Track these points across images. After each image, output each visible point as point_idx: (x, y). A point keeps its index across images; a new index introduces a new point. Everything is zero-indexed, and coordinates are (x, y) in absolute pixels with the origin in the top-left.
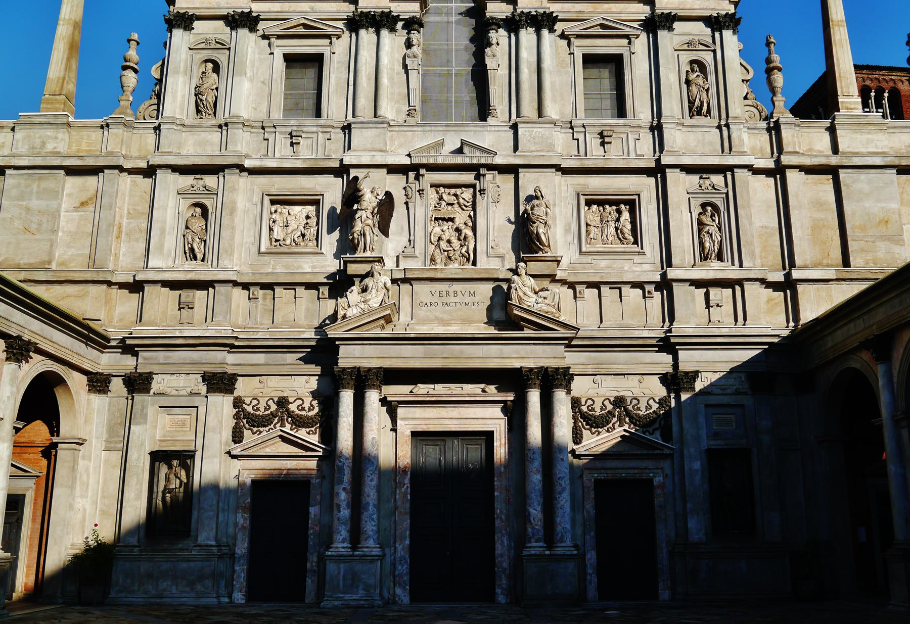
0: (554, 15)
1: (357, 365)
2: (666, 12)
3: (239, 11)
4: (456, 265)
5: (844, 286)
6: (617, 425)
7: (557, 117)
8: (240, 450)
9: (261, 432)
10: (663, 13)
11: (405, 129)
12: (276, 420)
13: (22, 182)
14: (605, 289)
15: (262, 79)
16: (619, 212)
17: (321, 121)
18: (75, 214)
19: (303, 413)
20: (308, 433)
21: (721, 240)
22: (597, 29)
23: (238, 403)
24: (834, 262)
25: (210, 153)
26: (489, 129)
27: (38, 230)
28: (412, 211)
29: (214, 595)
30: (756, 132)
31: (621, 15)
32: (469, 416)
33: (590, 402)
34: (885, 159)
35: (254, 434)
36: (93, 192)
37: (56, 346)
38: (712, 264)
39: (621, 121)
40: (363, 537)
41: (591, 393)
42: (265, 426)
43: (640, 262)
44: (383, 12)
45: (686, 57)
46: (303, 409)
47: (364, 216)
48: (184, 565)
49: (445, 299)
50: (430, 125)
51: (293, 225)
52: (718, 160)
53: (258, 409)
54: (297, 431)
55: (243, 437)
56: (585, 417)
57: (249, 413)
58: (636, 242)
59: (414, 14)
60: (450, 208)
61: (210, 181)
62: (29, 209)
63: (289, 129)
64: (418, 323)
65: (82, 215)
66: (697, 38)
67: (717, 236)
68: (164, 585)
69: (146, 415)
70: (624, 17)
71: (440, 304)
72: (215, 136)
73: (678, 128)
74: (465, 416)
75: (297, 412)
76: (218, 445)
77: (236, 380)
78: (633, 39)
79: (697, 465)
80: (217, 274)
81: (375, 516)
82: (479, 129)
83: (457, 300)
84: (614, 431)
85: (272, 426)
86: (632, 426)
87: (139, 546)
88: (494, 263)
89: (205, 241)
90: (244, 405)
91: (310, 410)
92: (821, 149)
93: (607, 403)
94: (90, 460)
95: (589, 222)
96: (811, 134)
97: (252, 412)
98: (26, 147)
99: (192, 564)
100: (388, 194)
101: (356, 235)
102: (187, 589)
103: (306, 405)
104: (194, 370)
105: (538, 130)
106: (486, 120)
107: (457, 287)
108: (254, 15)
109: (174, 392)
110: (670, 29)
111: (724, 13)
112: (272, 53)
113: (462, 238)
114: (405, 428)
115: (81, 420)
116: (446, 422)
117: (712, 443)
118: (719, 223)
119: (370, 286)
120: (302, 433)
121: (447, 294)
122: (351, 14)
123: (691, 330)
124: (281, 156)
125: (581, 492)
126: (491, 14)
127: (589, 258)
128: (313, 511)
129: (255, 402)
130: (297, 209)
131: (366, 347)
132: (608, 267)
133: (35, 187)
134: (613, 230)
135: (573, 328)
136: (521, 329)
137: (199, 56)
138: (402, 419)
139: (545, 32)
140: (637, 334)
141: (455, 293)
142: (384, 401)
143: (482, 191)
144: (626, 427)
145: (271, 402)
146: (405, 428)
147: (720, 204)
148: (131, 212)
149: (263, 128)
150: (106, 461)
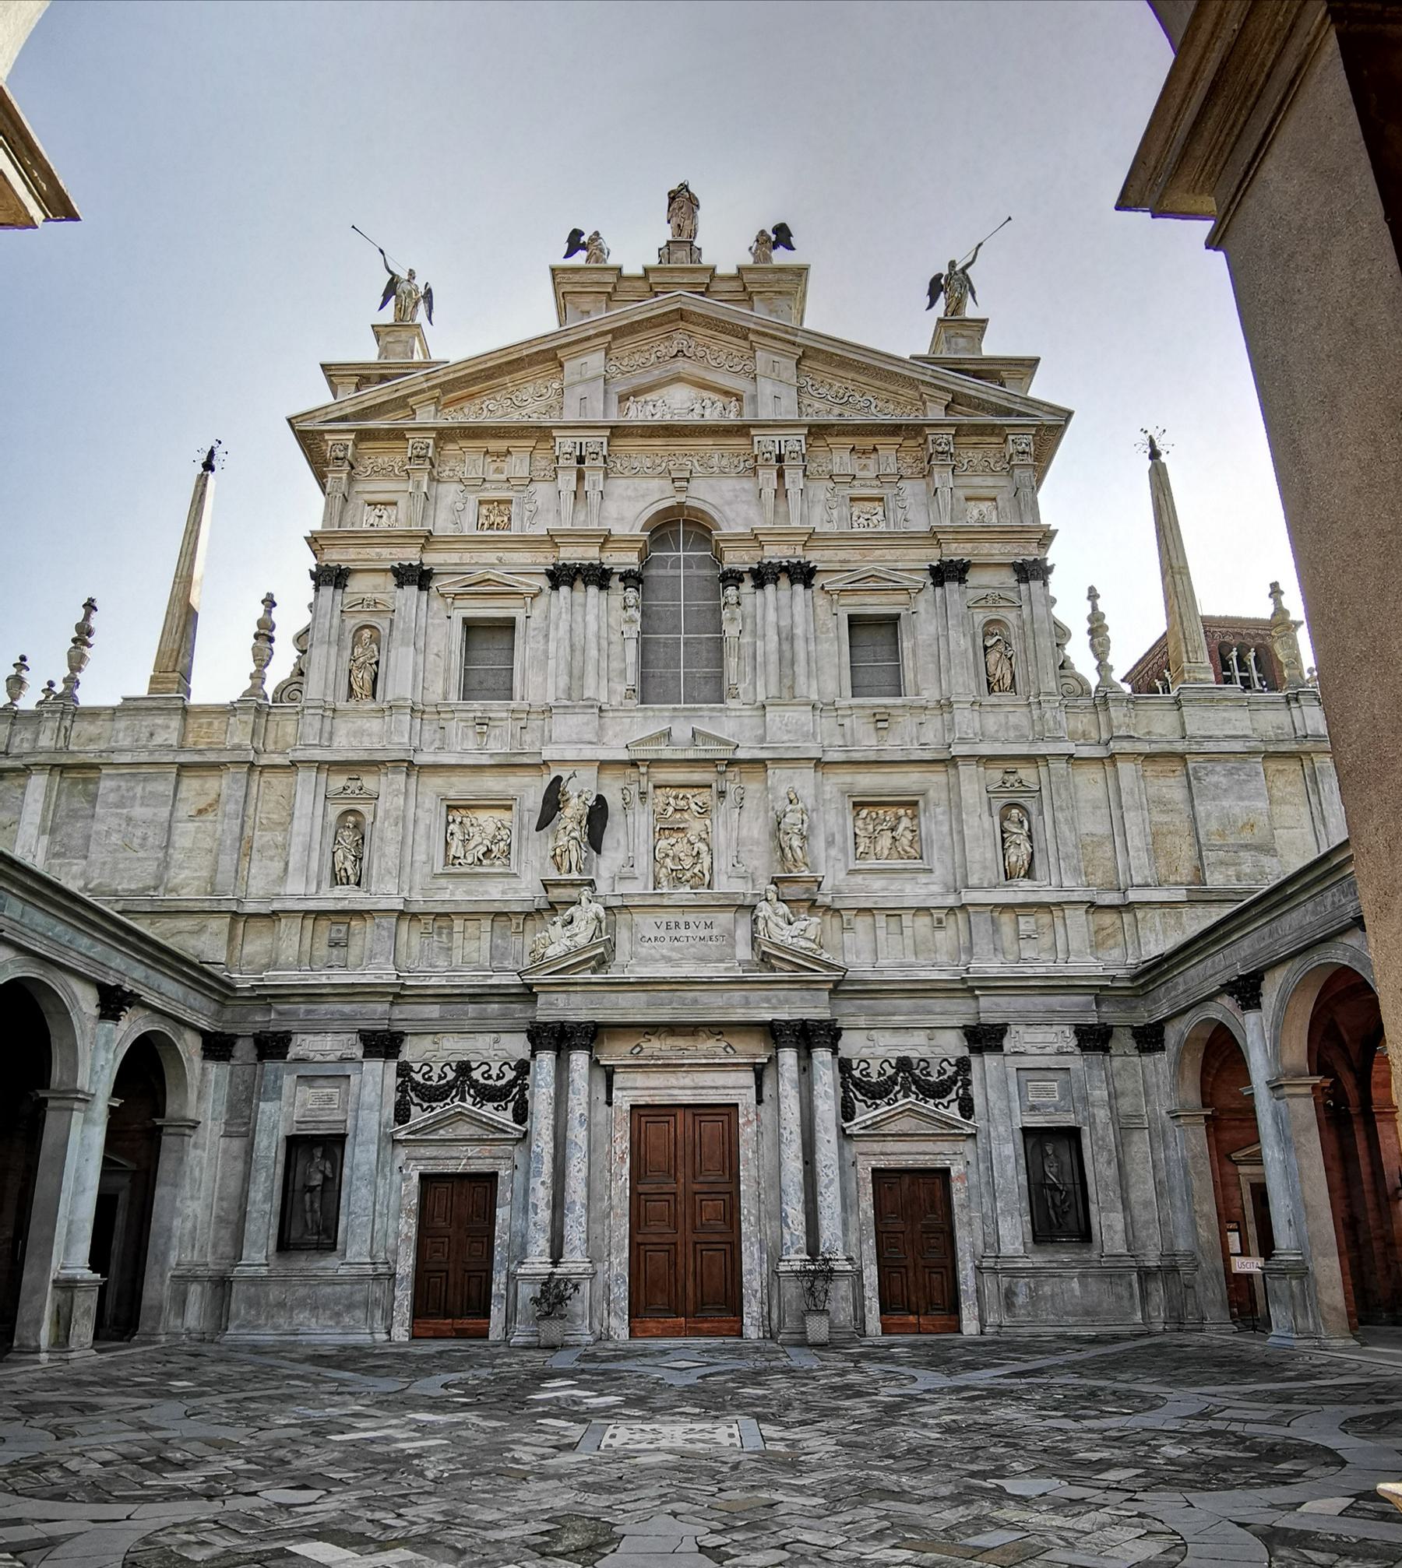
0: (811, 565)
1: (562, 1019)
2: (955, 559)
3: (407, 563)
4: (687, 889)
5: (1200, 910)
6: (899, 1096)
7: (816, 698)
8: (404, 1132)
9: (433, 1109)
10: (952, 561)
11: (621, 714)
12: (454, 1093)
13: (123, 784)
14: (881, 920)
15: (435, 651)
16: (899, 818)
17: (513, 705)
18: (190, 824)
19: (490, 1082)
20: (496, 1109)
21: (1032, 853)
23: (404, 1070)
24: (1184, 879)
25: (368, 745)
26: (728, 713)
27: (142, 846)
28: (630, 819)
29: (368, 1331)
32: (706, 1084)
33: (863, 1065)
34: (1247, 744)
35: (424, 1111)
36: (213, 796)
37: (164, 998)
38: (1021, 884)
39: (899, 701)
40: (566, 1249)
41: (865, 1053)
42: (441, 1101)
43: (924, 881)
44: (591, 565)
45: (980, 617)
46: (490, 1077)
47: (569, 827)
48: (329, 1290)
49: (673, 933)
50: (652, 710)
51: (477, 839)
53: (430, 1078)
54: (483, 1105)
55: (409, 1116)
56: (858, 1084)
57: (418, 1084)
58: (921, 858)
59: (631, 567)
60: (678, 815)
61: (369, 782)
62: (131, 819)
63: (472, 715)
64: (639, 964)
65: (200, 827)
67: (1026, 847)
68: (301, 1316)
69: (281, 1087)
70: (900, 565)
71: (668, 939)
72: (375, 725)
74: (701, 1084)
75: (482, 1081)
76: (377, 1128)
77: (402, 1041)
78: (913, 595)
79: (1008, 1150)
80: (376, 903)
81: (583, 1220)
82: (715, 714)
83: (689, 933)
84: (897, 1104)
85: (448, 1101)
86: (921, 1096)
87: (267, 1265)
88: (737, 887)
89: (361, 859)
90: (412, 1074)
91: (499, 1078)
93: (886, 1066)
94: (204, 1150)
95: (858, 831)
96: (1149, 713)
97: (422, 1081)
98: (129, 739)
99: (338, 1288)
100: (600, 799)
101: (558, 851)
102: (330, 1323)
103: (494, 1073)
104: (346, 1028)
105: (791, 714)
107: (691, 917)
108: (425, 568)
109: (319, 1058)
110: (962, 581)
111: (1031, 558)
112: (449, 617)
113: (694, 854)
114: (623, 1100)
115: (192, 1096)
116: (676, 1092)
117: (1026, 1119)
118: (1030, 830)
119: (577, 915)
120: (488, 1110)
121: (677, 925)
122: (552, 568)
123: (996, 970)
124: (462, 746)
125: (854, 1185)
126: (730, 566)
127: (859, 879)
128: (501, 1213)
129: (426, 1069)
130: (482, 816)
131: (572, 994)
132: (883, 890)
133: (139, 790)
134: (890, 841)
135: (839, 969)
136: (773, 969)
137: (353, 622)
138: (618, 1089)
139: (799, 588)
140: (923, 975)
141: (687, 924)
142: (595, 1063)
143: (722, 794)
144: (912, 1098)
145: (447, 1069)
146: (623, 1100)
147: (1032, 806)
148: (264, 821)
149: (439, 713)
150: (225, 1151)
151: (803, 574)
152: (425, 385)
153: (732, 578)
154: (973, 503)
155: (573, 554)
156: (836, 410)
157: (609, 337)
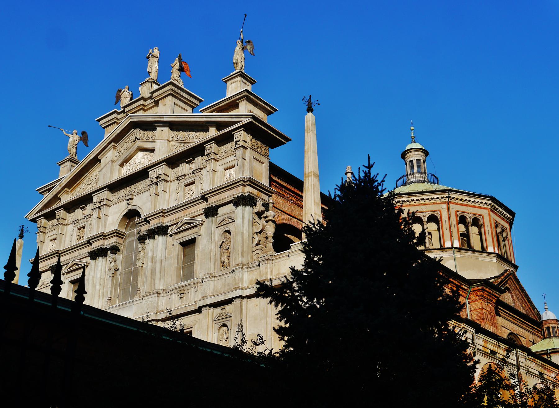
22: (186, 225)
30: (253, 269)
31: (195, 213)
52: (223, 297)
66: (226, 216)
70: (196, 214)
73: (211, 280)
92: (284, 272)
106: (134, 299)
151: (162, 230)
152: (60, 189)
153: (142, 239)
154: (228, 170)
155: (96, 245)
156: (183, 144)
157: (113, 143)
